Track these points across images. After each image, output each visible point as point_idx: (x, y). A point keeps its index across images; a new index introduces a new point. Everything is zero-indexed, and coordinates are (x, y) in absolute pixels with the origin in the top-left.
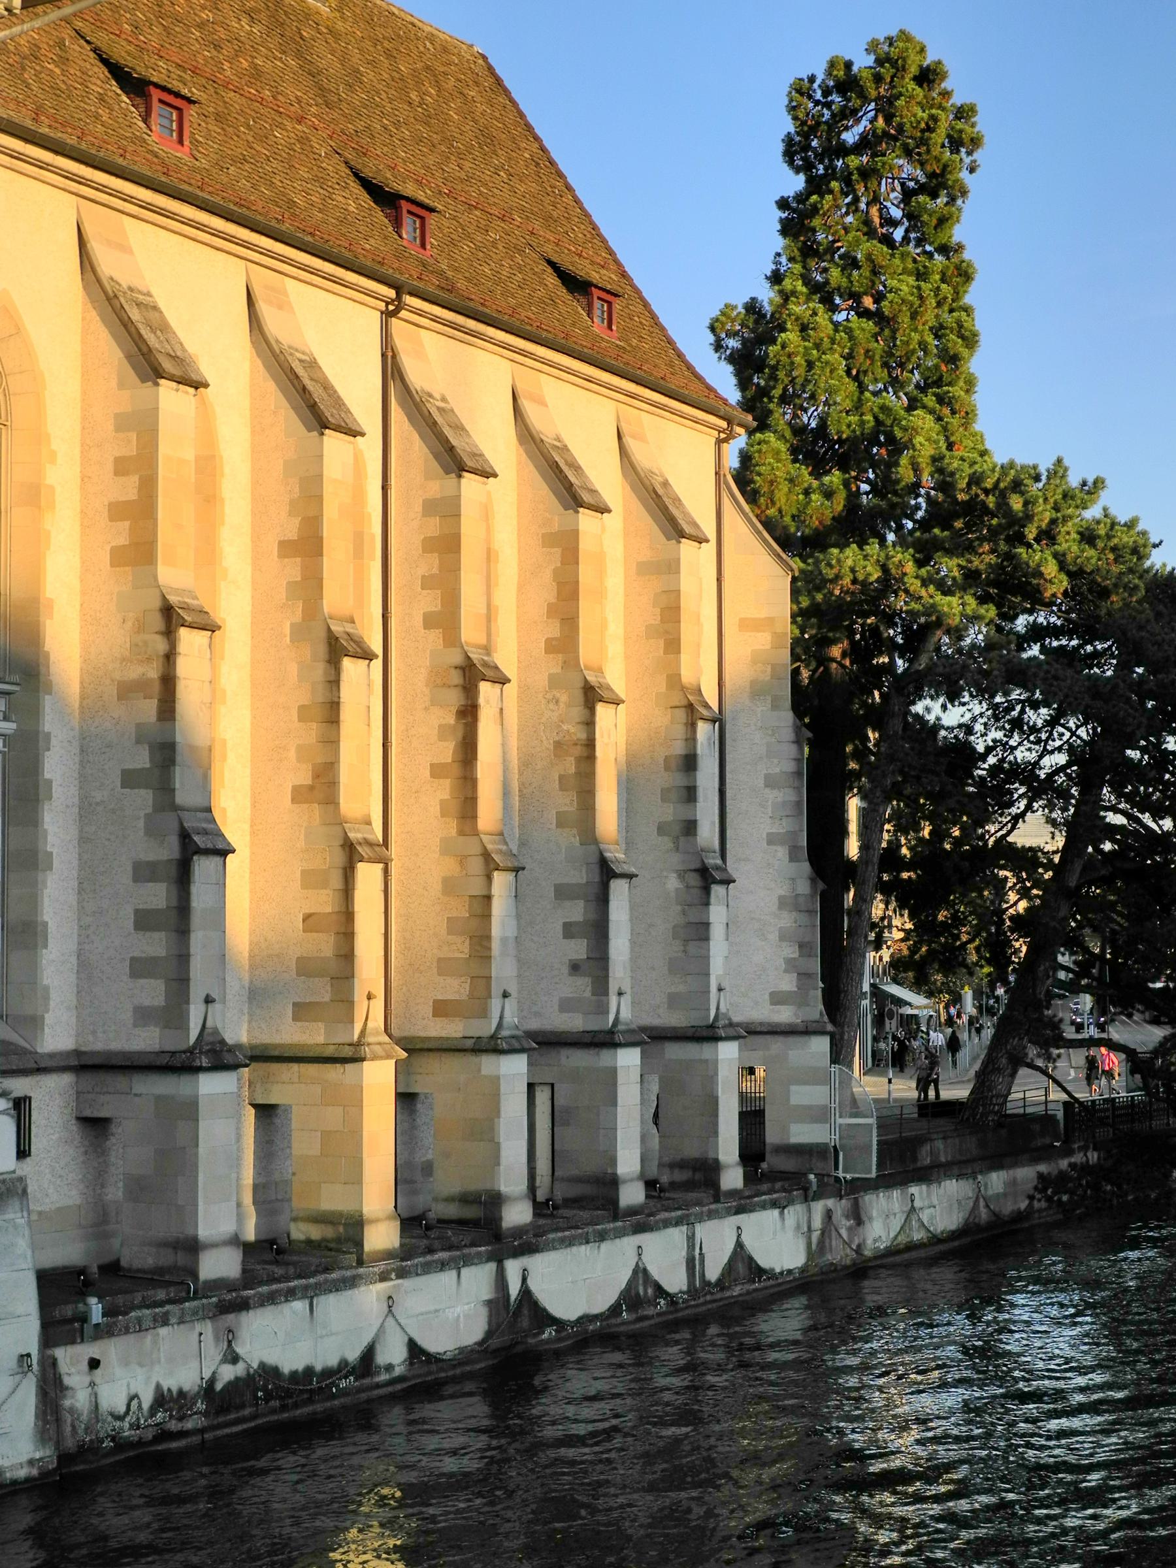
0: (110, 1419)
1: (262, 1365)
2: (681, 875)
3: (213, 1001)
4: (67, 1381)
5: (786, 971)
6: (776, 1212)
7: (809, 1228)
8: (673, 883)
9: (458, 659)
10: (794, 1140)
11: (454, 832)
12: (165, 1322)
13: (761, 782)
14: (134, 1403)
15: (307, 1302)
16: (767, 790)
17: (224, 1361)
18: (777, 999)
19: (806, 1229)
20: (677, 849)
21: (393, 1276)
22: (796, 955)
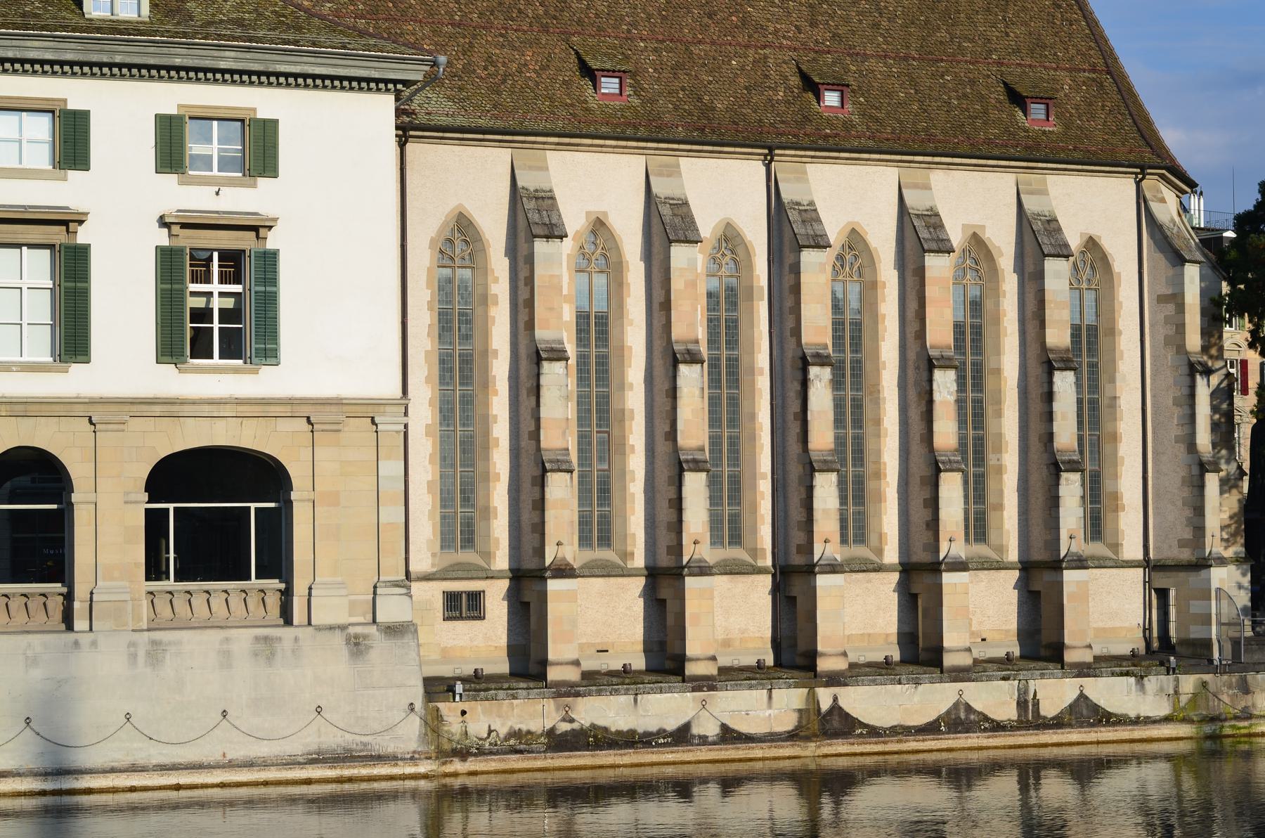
0: (475, 739)
1: (593, 726)
2: (1048, 466)
3: (562, 544)
4: (445, 718)
5: (1186, 526)
6: (1132, 680)
7: (1176, 692)
8: (1045, 471)
9: (800, 354)
10: (1192, 636)
11: (801, 450)
12: (515, 698)
13: (1170, 402)
14: (493, 734)
15: (632, 697)
16: (1175, 407)
17: (564, 720)
18: (1182, 544)
19: (1172, 692)
20: (1046, 451)
21: (705, 689)
22: (1192, 515)
